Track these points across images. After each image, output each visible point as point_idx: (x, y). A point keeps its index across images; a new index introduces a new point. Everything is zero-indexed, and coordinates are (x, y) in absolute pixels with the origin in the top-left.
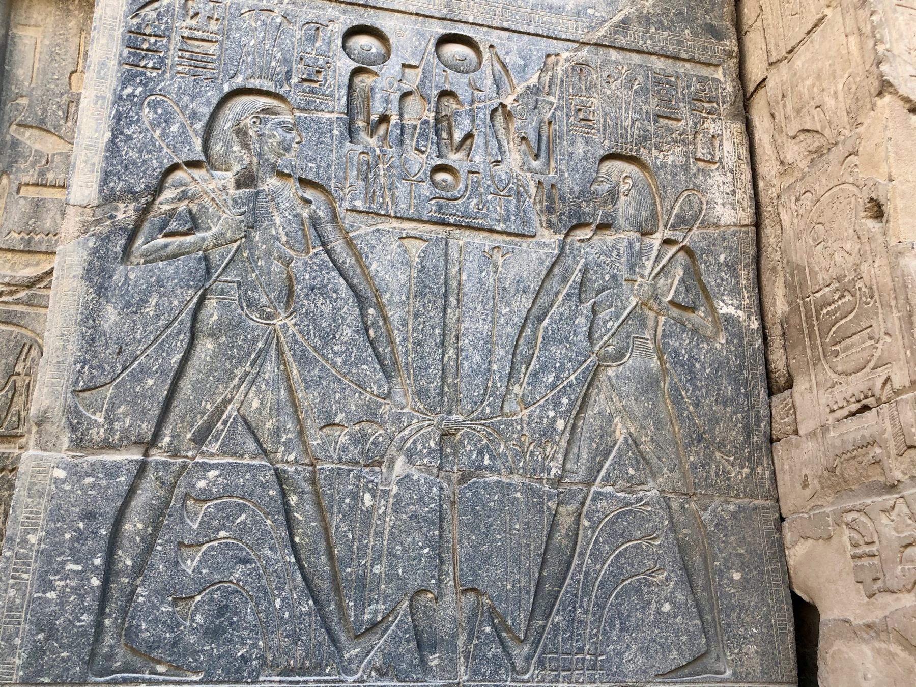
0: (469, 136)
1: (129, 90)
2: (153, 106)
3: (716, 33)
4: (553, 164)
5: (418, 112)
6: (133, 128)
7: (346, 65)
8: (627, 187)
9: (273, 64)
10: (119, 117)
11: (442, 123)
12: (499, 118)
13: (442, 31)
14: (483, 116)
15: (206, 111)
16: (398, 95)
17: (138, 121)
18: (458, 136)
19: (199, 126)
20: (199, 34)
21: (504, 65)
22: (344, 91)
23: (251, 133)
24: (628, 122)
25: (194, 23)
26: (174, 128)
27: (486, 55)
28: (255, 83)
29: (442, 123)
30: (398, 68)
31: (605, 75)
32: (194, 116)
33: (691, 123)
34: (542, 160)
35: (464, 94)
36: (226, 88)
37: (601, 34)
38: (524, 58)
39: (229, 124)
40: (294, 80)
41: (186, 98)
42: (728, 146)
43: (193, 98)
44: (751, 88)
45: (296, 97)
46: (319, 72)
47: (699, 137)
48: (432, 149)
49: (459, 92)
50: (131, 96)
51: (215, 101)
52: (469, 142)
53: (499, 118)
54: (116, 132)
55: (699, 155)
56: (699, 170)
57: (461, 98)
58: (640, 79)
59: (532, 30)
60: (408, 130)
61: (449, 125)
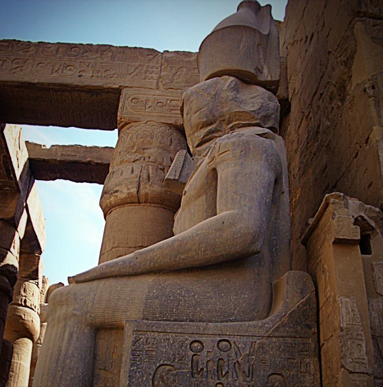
0: (227, 372)
1: (133, 368)
2: (139, 372)
3: (309, 327)
4: (253, 379)
5: (212, 366)
6: (134, 379)
7: (191, 353)
8: (277, 384)
9: (171, 356)
10: (130, 376)
11: (219, 369)
12: (237, 365)
13: (219, 339)
14: (232, 366)
15: (153, 372)
16: (206, 361)
17: (135, 377)
18: (224, 373)
19: (151, 377)
20: (150, 349)
21: (238, 348)
22: (190, 362)
23: (165, 378)
24: (278, 363)
25: (149, 346)
26: (144, 378)
27: (233, 345)
28: (166, 362)
29: (219, 369)
30: (206, 353)
31: (270, 347)
32: (150, 374)
33: (299, 360)
34: (250, 377)
35: (226, 359)
36: (158, 365)
37: (270, 333)
38: (244, 345)
39: (159, 376)
40: (176, 361)
41: (147, 369)
42: (312, 366)
43: (149, 369)
44: (321, 345)
45: (177, 366)
46: (183, 357)
47: (302, 364)
48: (216, 378)
49: (224, 358)
50: (133, 370)
51: (155, 369)
52: (227, 374)
53: (237, 365)
54: (130, 381)
55: (302, 371)
56: (302, 376)
57: (225, 360)
58: (282, 347)
59: (247, 334)
60: (209, 372)
61: (221, 368)
